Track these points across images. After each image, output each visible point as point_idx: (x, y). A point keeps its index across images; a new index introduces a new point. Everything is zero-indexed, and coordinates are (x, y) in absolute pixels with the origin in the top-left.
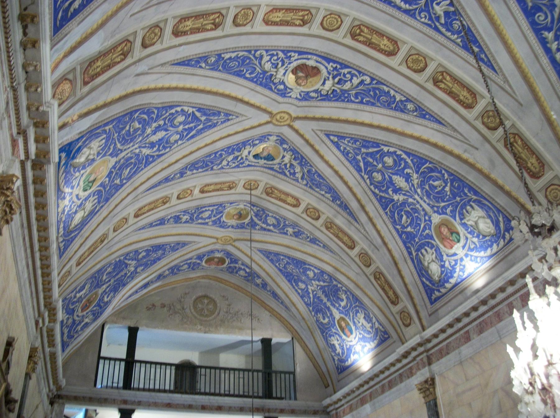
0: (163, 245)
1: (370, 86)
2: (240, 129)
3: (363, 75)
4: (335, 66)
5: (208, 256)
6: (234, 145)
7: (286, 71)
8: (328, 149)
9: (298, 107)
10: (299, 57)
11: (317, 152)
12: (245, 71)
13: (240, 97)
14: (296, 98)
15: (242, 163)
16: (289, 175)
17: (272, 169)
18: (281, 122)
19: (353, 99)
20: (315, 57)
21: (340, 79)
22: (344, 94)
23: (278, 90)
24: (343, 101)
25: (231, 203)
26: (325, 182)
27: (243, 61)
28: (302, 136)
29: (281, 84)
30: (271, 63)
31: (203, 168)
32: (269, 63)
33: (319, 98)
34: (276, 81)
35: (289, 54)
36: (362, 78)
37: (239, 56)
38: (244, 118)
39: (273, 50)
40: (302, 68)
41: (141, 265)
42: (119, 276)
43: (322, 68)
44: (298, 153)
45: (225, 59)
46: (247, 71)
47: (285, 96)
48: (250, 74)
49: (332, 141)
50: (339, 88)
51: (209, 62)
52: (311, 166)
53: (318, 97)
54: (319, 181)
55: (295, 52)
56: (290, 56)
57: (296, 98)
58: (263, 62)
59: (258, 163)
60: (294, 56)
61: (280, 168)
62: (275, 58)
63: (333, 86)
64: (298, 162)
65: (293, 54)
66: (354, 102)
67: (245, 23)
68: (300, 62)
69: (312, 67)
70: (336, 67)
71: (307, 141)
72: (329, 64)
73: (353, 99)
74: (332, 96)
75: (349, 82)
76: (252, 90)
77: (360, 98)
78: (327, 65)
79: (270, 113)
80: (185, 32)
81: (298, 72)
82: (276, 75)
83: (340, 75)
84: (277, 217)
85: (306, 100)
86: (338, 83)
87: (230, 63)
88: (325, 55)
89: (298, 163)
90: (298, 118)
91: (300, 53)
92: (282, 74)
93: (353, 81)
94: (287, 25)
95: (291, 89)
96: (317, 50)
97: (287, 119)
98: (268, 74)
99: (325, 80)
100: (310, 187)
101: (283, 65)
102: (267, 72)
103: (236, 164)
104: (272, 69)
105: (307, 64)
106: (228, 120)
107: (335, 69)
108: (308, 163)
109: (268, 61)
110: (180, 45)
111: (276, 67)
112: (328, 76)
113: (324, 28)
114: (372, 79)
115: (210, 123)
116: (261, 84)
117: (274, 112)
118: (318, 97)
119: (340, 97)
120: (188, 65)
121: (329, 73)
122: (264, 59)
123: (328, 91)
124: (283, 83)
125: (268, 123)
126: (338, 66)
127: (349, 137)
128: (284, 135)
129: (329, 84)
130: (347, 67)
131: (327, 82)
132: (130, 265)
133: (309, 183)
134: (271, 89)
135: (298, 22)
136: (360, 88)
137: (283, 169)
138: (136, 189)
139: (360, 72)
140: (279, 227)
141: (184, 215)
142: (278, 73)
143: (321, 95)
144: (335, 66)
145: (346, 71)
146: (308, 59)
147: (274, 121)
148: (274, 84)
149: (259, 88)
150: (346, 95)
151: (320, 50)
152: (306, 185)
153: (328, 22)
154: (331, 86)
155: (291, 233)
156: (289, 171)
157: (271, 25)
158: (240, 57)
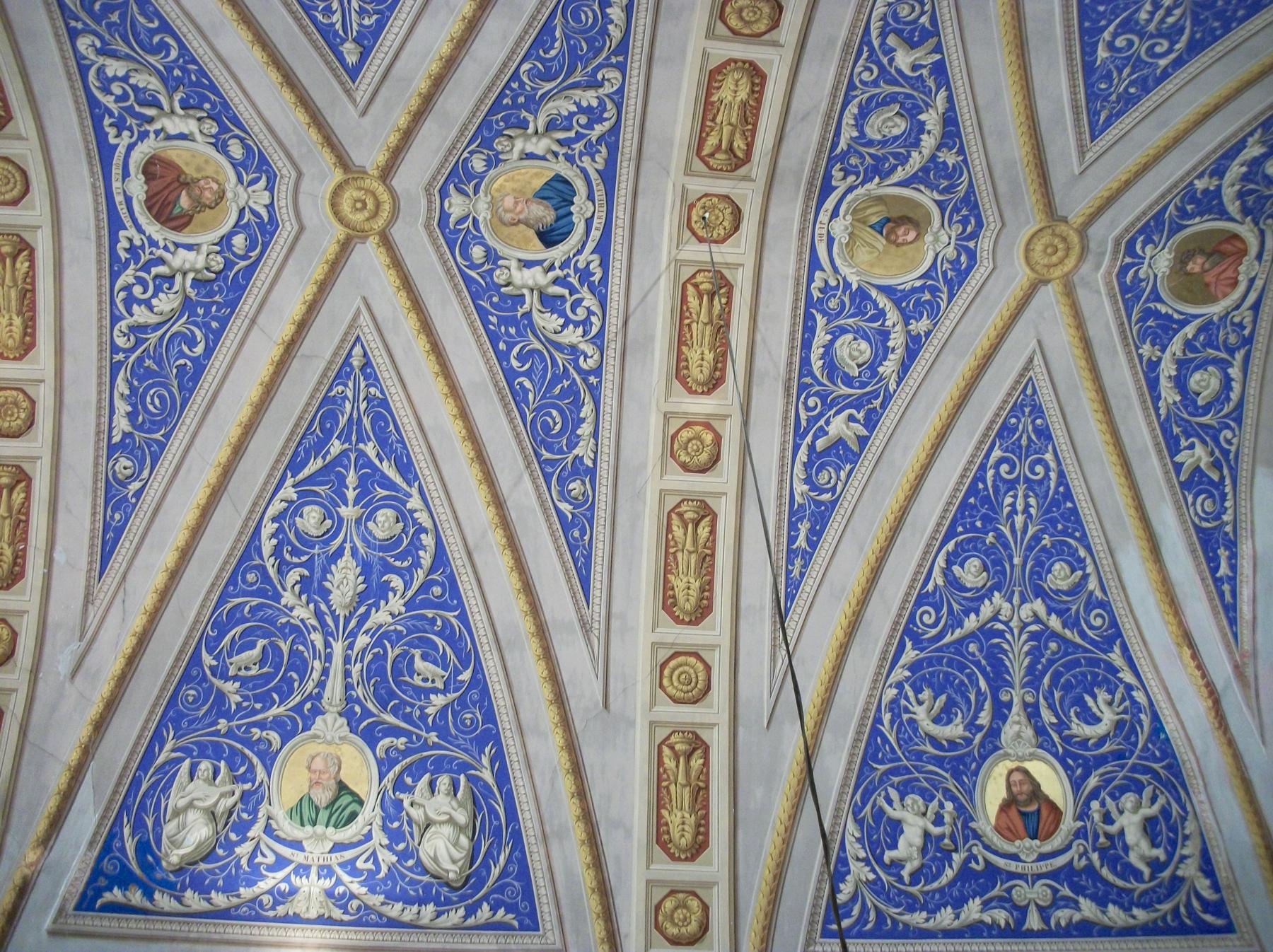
0: (972, 491)
1: (102, 30)
2: (410, 323)
3: (85, 58)
4: (112, 132)
5: (1159, 299)
6: (485, 323)
7: (177, 245)
8: (404, 55)
9: (300, 175)
10: (128, 222)
11: (439, 82)
12: (182, 362)
13: (276, 352)
14: (270, 188)
15: (585, 275)
16: (607, 125)
17: (609, 176)
18: (378, 205)
19: (174, 54)
20: (116, 185)
21: (141, 104)
22: (177, 79)
23: (251, 248)
24: (202, 72)
25: (815, 264)
26: (558, 20)
27: (149, 373)
28: (407, 136)
29: (230, 246)
30: (155, 295)
31: (577, 404)
32: (154, 302)
33: (237, 132)
34: (218, 263)
35: (123, 255)
36: (92, 57)
37: (127, 392)
38: (365, 319)
39: (113, 302)
40: (161, 208)
41: (1041, 569)
42: (1017, 666)
43: (138, 156)
44: (485, 123)
45: (128, 429)
46: (182, 355)
47: (272, 218)
48: (192, 343)
49: (364, 56)
50: (171, 98)
51: (129, 472)
52: (515, 76)
53: (236, 137)
54: (567, 38)
55: (114, 240)
56: (132, 250)
57: (270, 188)
58: (153, 319)
59: (589, 222)
60: (130, 240)
61: (591, 151)
62: (137, 290)
63: (173, 112)
64: (524, 114)
65: (124, 244)
66: (182, 46)
67: (25, 405)
68: (143, 218)
69: (147, 182)
70: (111, 125)
71: (418, 117)
72: (116, 146)
73: (174, 54)
74: (207, 106)
75: (132, 81)
76: (253, 321)
77: (156, 39)
78: (121, 150)
79: (345, 247)
80: (16, 557)
81: (177, 211)
82: (197, 271)
83: (130, 110)
84: (853, 109)
85: (263, 160)
86: (156, 104)
87: (146, 410)
88: (97, 162)
89: (535, 114)
90: (343, 161)
91: (115, 224)
92: (191, 255)
93: (121, 73)
94: (33, 291)
95: (242, 211)
96: (94, 186)
97: (360, 189)
98: (192, 293)
99: (169, 138)
100: (623, 47)
101: (161, 261)
102: (187, 298)
103: (585, 292)
104: (176, 287)
105: (143, 197)
106: (367, 364)
107: (120, 126)
108: (507, 86)
109: (151, 308)
110: (49, 562)
111: (171, 279)
112: (152, 136)
113: (26, 190)
114: (73, 35)
115: (366, 422)
116: (233, 305)
117: (340, 232)
118: (236, 137)
119: (198, 84)
120: (119, 531)
121: (143, 136)
122: (141, 320)
123: (199, 119)
124: (225, 242)
125: (386, 241)
126: (107, 121)
127: (314, 20)
128: (434, 178)
129: (174, 125)
130: (93, 102)
131: (172, 130)
132: (995, 618)
133: (600, 60)
134: (250, 271)
135: (22, 266)
136: (128, 51)
137: (589, 144)
138: (542, 631)
139: (83, 70)
140: (908, 96)
141: (822, 432)
142: (187, 266)
143: (223, 129)
144: (112, 132)
145: (108, 101)
146: (128, 200)
147: (380, 222)
148: (229, 264)
149: (248, 305)
150: (177, 72)
151: (88, 181)
152: (622, 68)
153: (11, 185)
154: (177, 120)
155: (918, 54)
156: (590, 126)
157: (33, 335)
158: (131, 387)
